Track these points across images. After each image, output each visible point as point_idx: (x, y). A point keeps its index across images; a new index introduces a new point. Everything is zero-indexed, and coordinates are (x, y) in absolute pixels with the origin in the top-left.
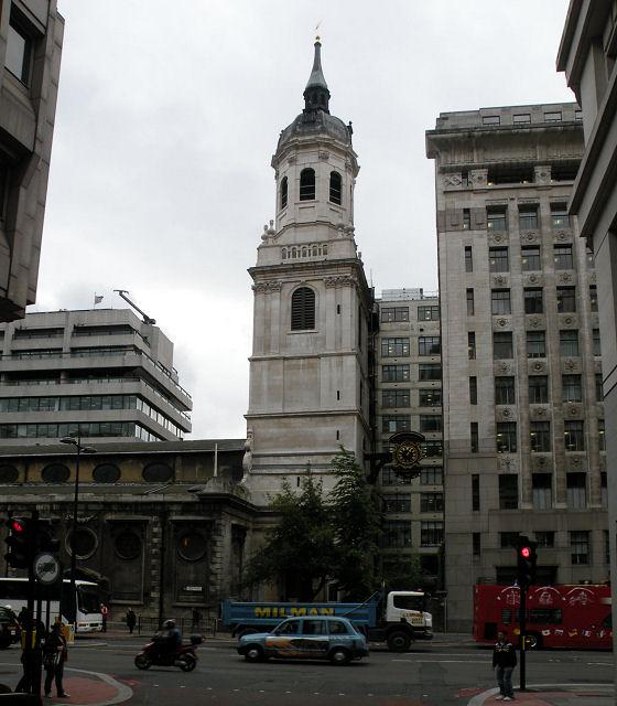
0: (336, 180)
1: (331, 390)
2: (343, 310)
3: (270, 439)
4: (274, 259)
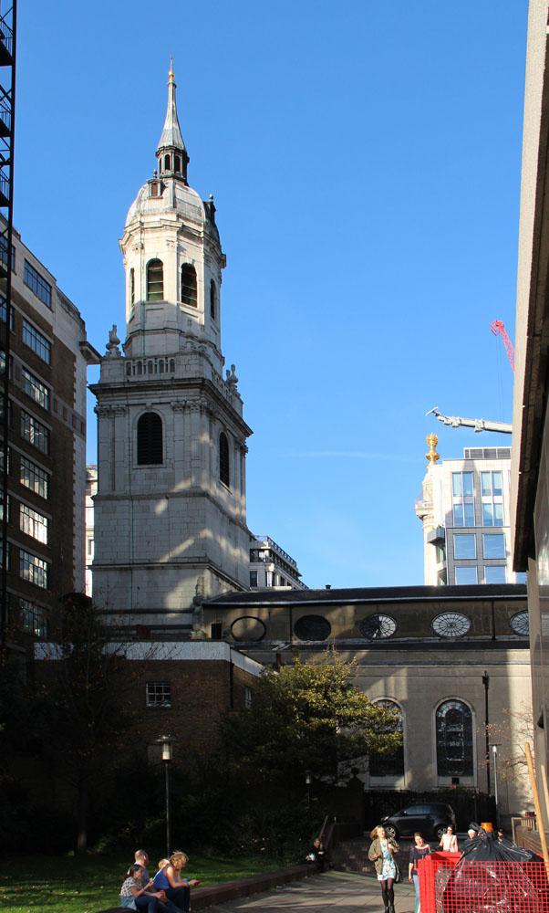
0: (188, 273)
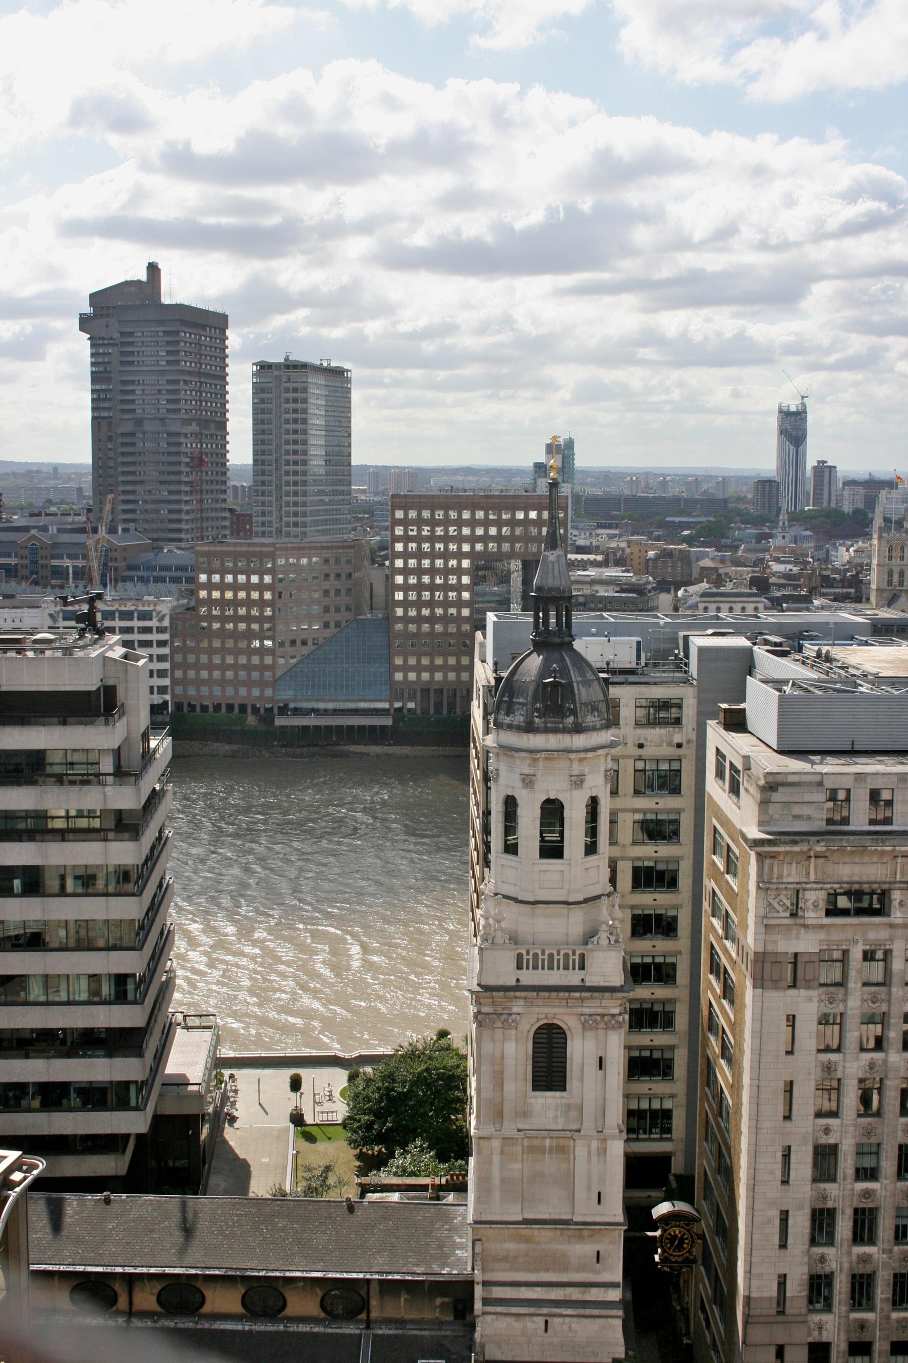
1: (589, 1188)
2: (608, 1063)
3: (505, 1259)
4: (505, 973)
